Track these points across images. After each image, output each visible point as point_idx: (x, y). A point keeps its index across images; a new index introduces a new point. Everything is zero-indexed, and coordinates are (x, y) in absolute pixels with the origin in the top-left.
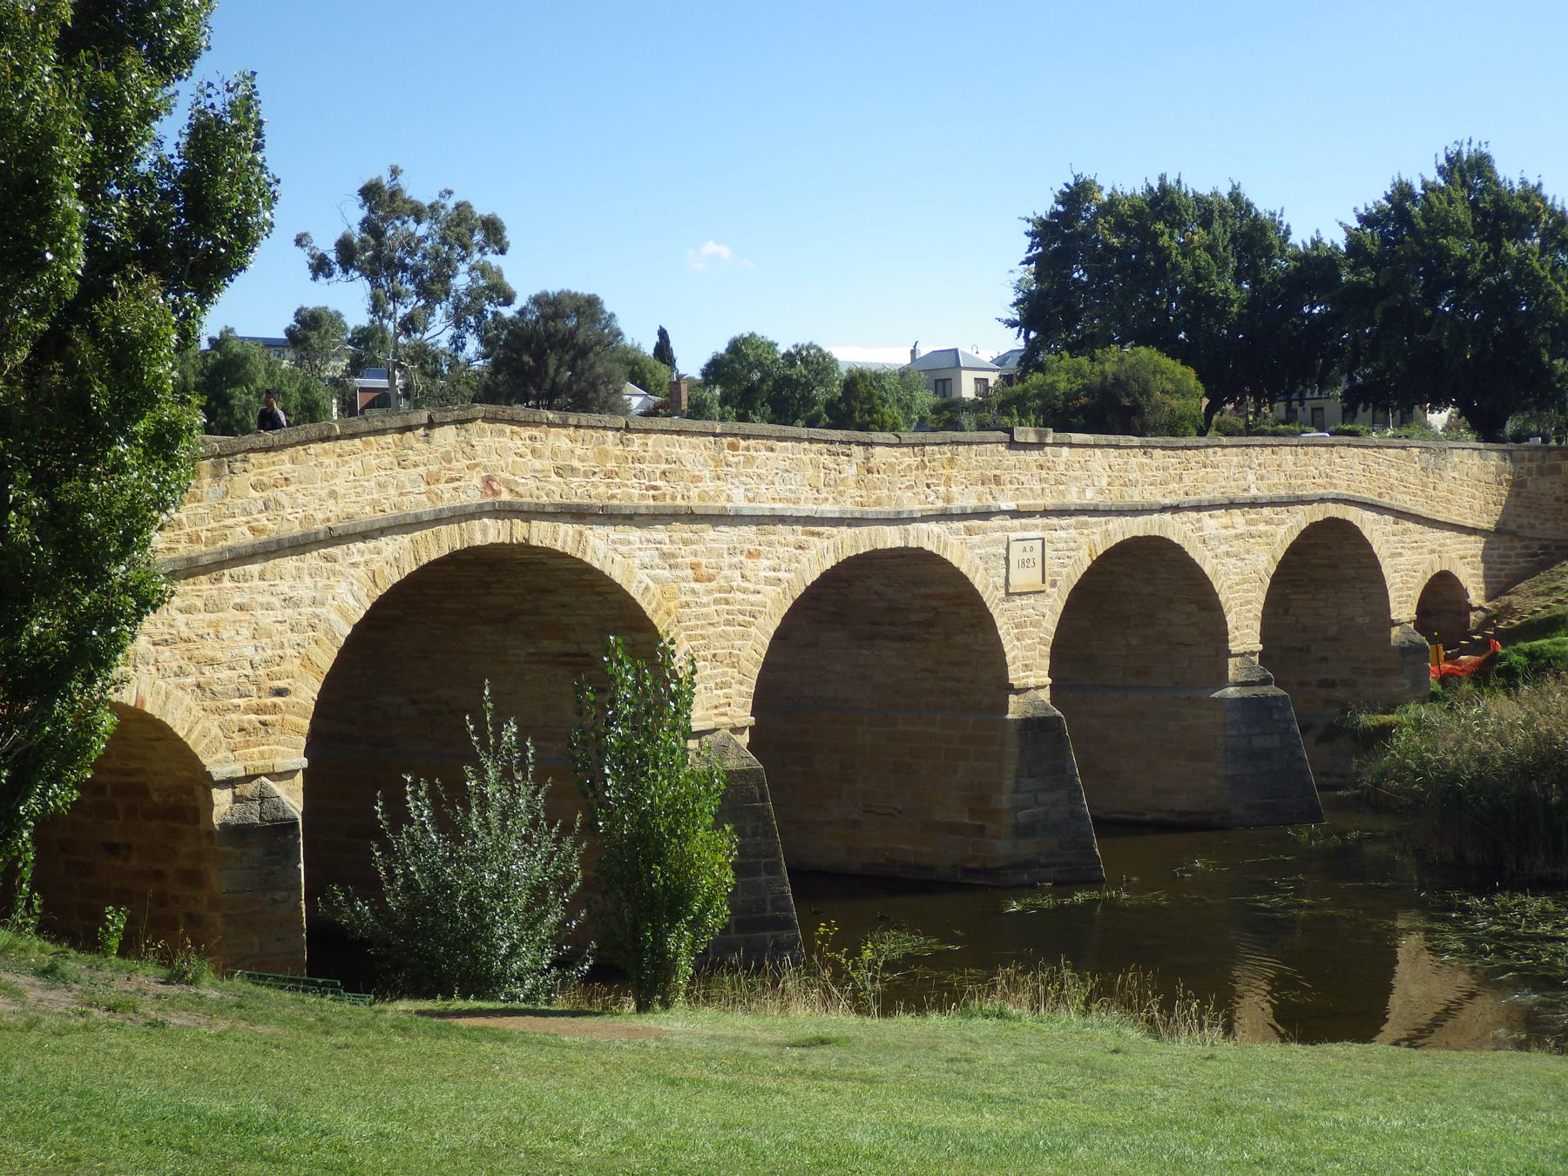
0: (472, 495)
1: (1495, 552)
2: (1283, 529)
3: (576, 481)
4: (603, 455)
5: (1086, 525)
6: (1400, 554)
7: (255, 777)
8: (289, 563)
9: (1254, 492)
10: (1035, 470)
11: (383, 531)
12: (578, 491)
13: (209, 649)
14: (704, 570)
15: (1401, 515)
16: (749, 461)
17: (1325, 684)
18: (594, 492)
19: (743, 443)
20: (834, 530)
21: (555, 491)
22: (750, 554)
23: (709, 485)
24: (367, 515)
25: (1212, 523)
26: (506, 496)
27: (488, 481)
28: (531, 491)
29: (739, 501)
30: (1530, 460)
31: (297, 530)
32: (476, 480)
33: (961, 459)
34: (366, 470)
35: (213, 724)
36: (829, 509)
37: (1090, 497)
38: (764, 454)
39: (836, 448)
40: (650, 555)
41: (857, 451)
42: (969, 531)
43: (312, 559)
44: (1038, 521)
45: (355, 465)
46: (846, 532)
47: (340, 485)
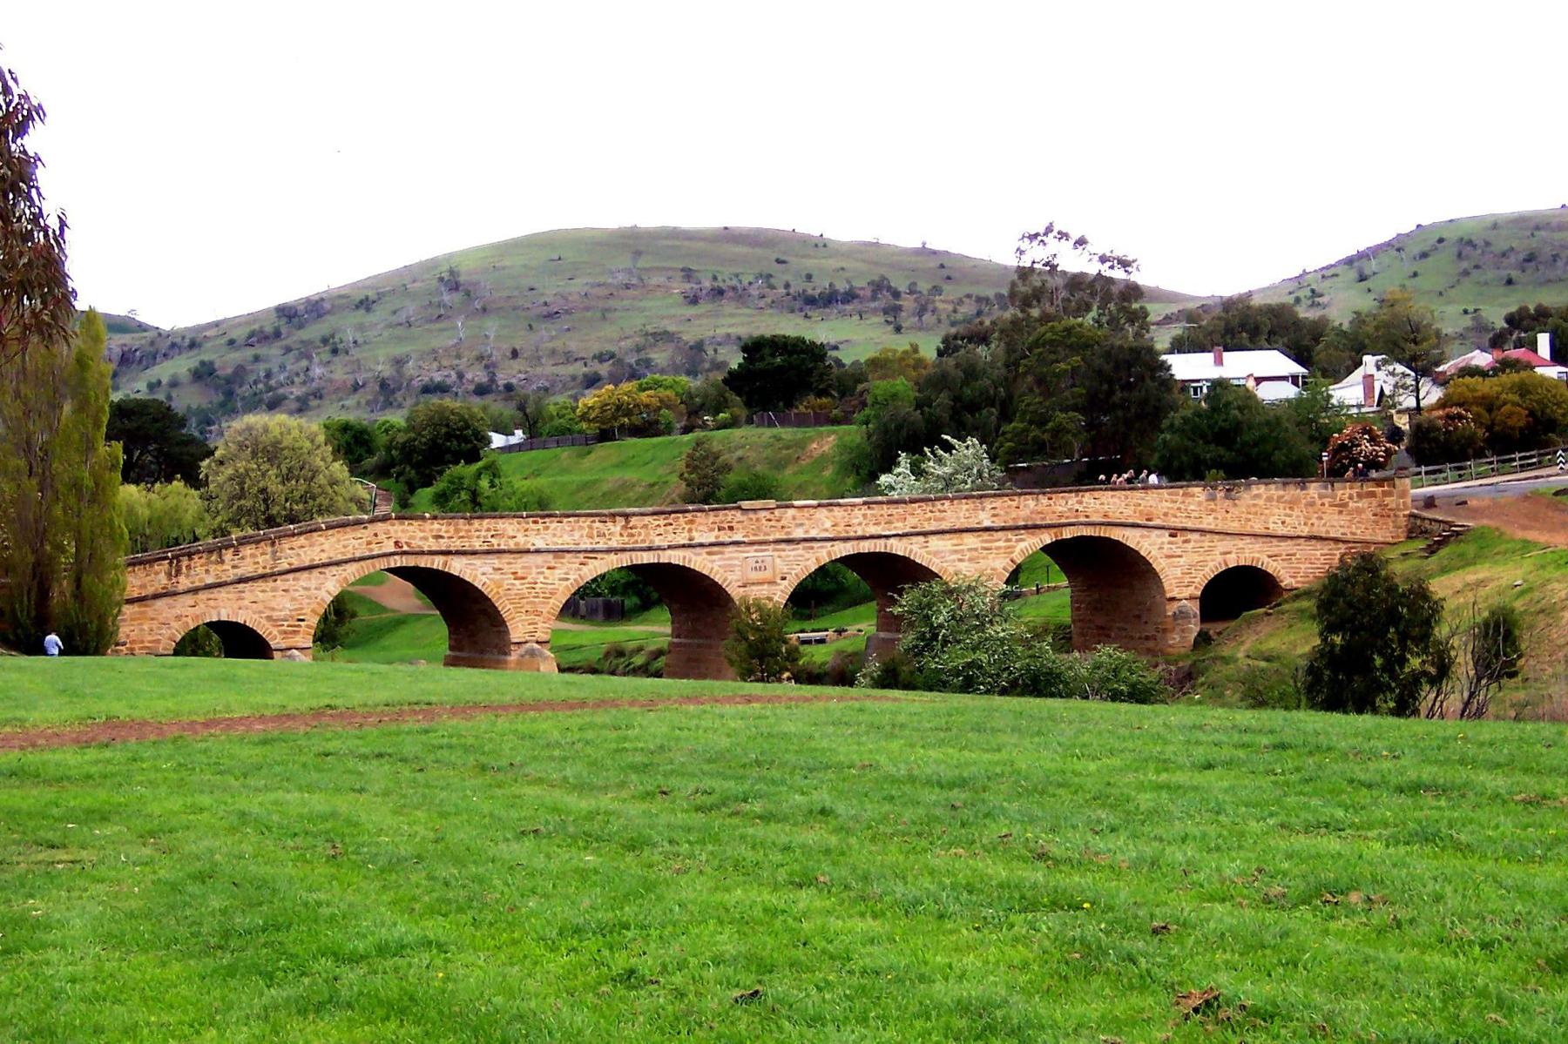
0: (389, 547)
1: (1318, 553)
2: (1022, 545)
3: (442, 541)
4: (457, 531)
5: (812, 548)
6: (1180, 556)
7: (290, 649)
8: (305, 575)
9: (987, 523)
10: (764, 521)
11: (346, 562)
12: (443, 545)
13: (273, 604)
14: (519, 575)
15: (1174, 532)
16: (547, 528)
17: (1147, 638)
18: (456, 544)
19: (565, 520)
20: (605, 556)
21: (431, 545)
22: (549, 568)
23: (521, 539)
24: (340, 557)
25: (935, 543)
26: (405, 548)
27: (396, 543)
28: (417, 544)
29: (540, 545)
30: (1351, 488)
31: (307, 564)
32: (391, 542)
33: (698, 520)
34: (339, 541)
35: (275, 632)
36: (601, 546)
37: (813, 534)
38: (555, 524)
39: (603, 519)
40: (488, 569)
41: (621, 521)
42: (709, 553)
43: (315, 572)
44: (772, 546)
45: (333, 540)
46: (612, 556)
47: (326, 547)
